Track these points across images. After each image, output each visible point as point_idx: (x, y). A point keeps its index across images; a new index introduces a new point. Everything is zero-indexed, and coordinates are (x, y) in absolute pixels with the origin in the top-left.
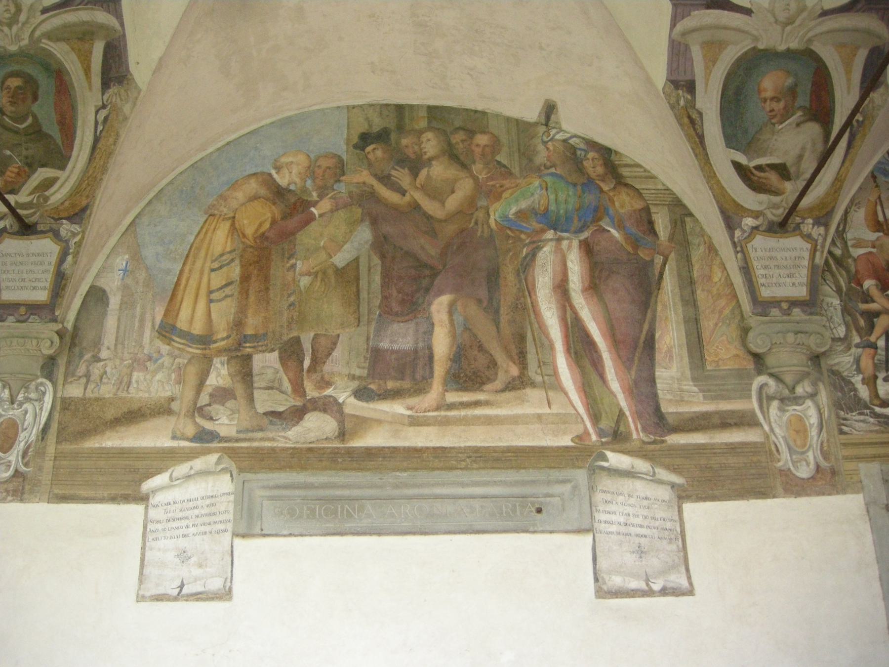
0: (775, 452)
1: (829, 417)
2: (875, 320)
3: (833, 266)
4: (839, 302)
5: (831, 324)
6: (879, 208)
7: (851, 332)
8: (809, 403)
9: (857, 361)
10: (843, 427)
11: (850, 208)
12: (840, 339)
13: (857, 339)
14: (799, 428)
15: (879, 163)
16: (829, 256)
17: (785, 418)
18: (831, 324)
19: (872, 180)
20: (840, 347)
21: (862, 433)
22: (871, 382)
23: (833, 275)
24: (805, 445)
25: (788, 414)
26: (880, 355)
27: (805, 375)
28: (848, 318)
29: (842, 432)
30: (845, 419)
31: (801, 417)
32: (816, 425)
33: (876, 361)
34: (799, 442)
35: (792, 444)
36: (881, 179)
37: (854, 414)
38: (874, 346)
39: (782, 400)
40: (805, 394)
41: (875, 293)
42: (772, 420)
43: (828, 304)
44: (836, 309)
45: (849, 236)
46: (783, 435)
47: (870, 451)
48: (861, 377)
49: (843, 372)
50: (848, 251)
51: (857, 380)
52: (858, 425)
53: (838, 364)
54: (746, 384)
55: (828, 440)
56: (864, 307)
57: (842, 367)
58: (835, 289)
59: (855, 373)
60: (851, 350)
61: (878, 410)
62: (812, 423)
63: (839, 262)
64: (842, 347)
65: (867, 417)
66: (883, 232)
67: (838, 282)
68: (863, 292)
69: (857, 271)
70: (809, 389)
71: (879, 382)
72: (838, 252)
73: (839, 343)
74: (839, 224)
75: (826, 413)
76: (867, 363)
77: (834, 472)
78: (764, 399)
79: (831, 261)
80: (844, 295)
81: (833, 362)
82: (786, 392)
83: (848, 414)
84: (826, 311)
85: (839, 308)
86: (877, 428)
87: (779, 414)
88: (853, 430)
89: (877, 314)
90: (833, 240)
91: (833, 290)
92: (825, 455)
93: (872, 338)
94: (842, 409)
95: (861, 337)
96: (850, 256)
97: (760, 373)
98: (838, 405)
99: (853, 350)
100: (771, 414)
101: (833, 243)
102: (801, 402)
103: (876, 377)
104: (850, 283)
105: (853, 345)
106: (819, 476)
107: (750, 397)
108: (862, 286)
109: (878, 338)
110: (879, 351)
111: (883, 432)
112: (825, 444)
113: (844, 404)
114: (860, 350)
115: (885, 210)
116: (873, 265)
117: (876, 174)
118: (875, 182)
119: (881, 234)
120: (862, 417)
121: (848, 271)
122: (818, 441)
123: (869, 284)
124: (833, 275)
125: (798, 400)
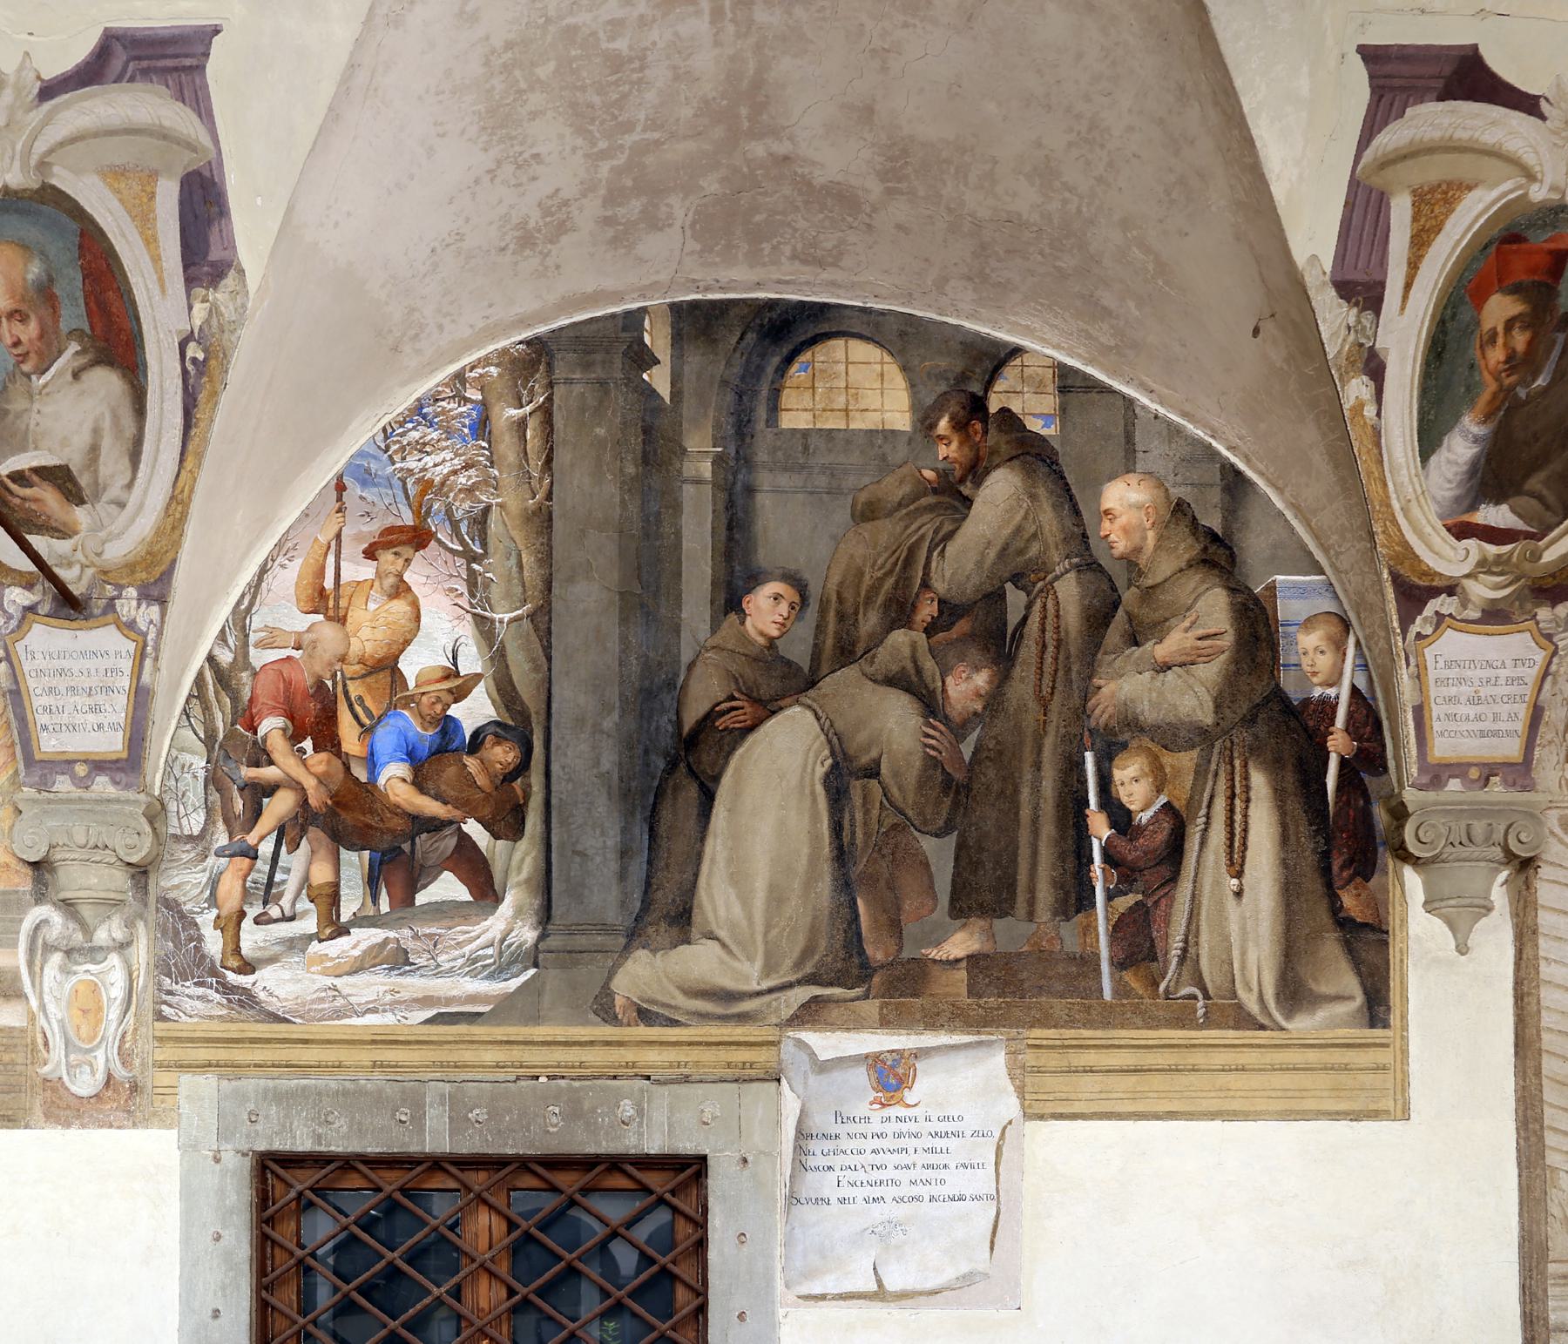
0: (41, 1047)
1: (145, 987)
2: (266, 800)
3: (211, 687)
4: (204, 764)
5: (181, 806)
6: (331, 559)
7: (214, 823)
8: (114, 959)
9: (214, 883)
10: (164, 1007)
11: (273, 561)
12: (191, 838)
13: (222, 839)
14: (89, 1005)
15: (361, 454)
16: (207, 665)
17: (68, 986)
18: (181, 806)
19: (334, 495)
20: (186, 853)
21: (195, 1020)
22: (231, 925)
23: (206, 708)
24: (95, 1036)
25: (74, 979)
26: (259, 871)
27: (117, 904)
28: (215, 797)
29: (160, 1017)
30: (170, 993)
31: (96, 984)
32: (118, 1002)
33: (248, 884)
34: (84, 1031)
35: (72, 1034)
36: (354, 490)
37: (188, 984)
38: (252, 854)
39: (68, 952)
40: (111, 943)
41: (278, 746)
42: (46, 989)
43: (183, 767)
44: (196, 777)
45: (256, 622)
46: (59, 1016)
47: (203, 1054)
48: (215, 912)
49: (185, 903)
50: (246, 655)
51: (206, 920)
52: (188, 1004)
53: (177, 887)
54: (11, 921)
55: (136, 1030)
56: (248, 773)
57: (184, 895)
58: (202, 735)
59: (206, 905)
60: (208, 860)
61: (231, 977)
62: (112, 996)
63: (224, 678)
64: (193, 855)
65: (209, 991)
66: (325, 615)
67: (213, 720)
68: (255, 743)
69: (251, 700)
70: (119, 934)
71: (247, 924)
72: (225, 657)
73: (188, 847)
74: (243, 596)
75: (141, 979)
76: (230, 889)
77: (135, 1088)
78: (39, 948)
79: (209, 676)
80: (217, 746)
81: (169, 885)
82: (79, 937)
83: (177, 983)
84: (177, 780)
85: (201, 774)
86: (225, 1012)
87: (58, 977)
88: (181, 1014)
89: (270, 789)
90: (223, 631)
91: (200, 738)
92: (125, 1057)
93: (251, 839)
94: (169, 975)
95: (231, 838)
96: (247, 665)
97: (40, 899)
98: (163, 967)
99: (211, 860)
100: (46, 978)
101: (222, 637)
102: (99, 956)
103: (242, 914)
104: (232, 725)
105: (213, 852)
106: (110, 1093)
107: (15, 945)
108: (255, 733)
109: (262, 838)
110: (259, 863)
111: (232, 1021)
112: (128, 1037)
113: (175, 964)
114: (224, 860)
115: (342, 563)
116: (288, 684)
117: (346, 480)
118: (339, 499)
119: (320, 617)
120: (201, 991)
121: (235, 699)
122: (117, 1030)
123: (271, 726)
124: (206, 708)
125: (94, 953)
